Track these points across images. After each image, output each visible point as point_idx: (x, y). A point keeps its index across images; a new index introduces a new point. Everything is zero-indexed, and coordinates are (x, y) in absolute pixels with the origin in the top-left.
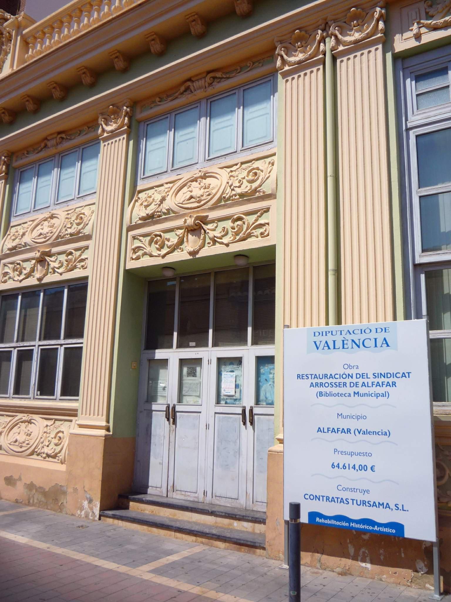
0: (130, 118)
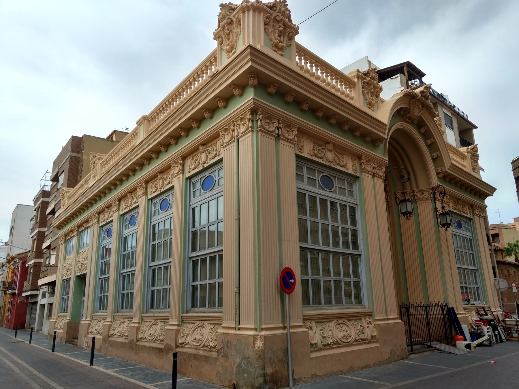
0: (253, 121)
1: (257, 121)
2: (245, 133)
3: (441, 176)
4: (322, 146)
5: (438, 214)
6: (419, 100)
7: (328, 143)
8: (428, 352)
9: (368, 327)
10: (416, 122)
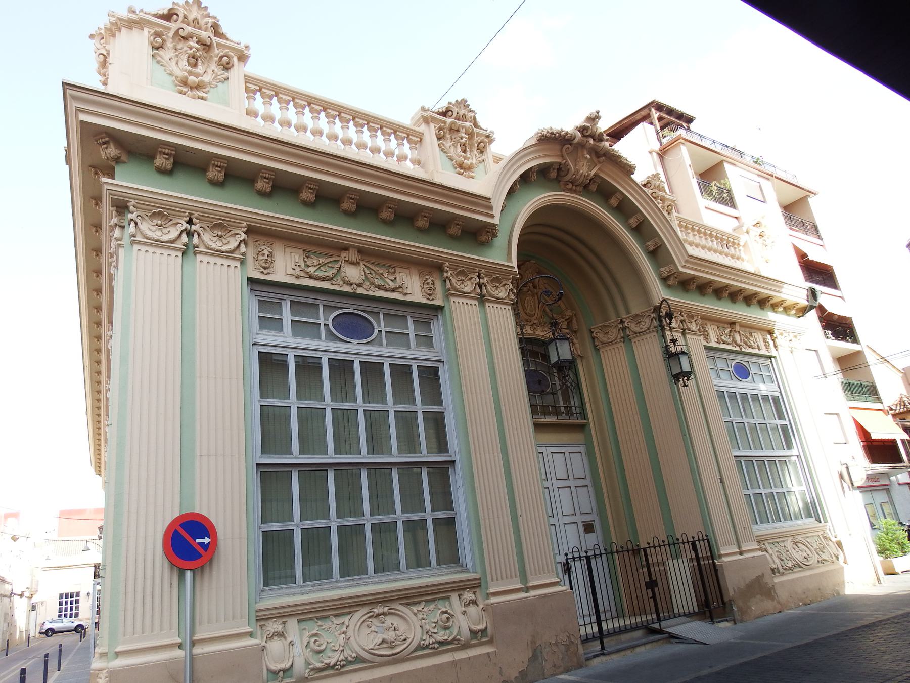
4: (331, 256)
7: (346, 248)
8: (648, 646)
9: (464, 613)
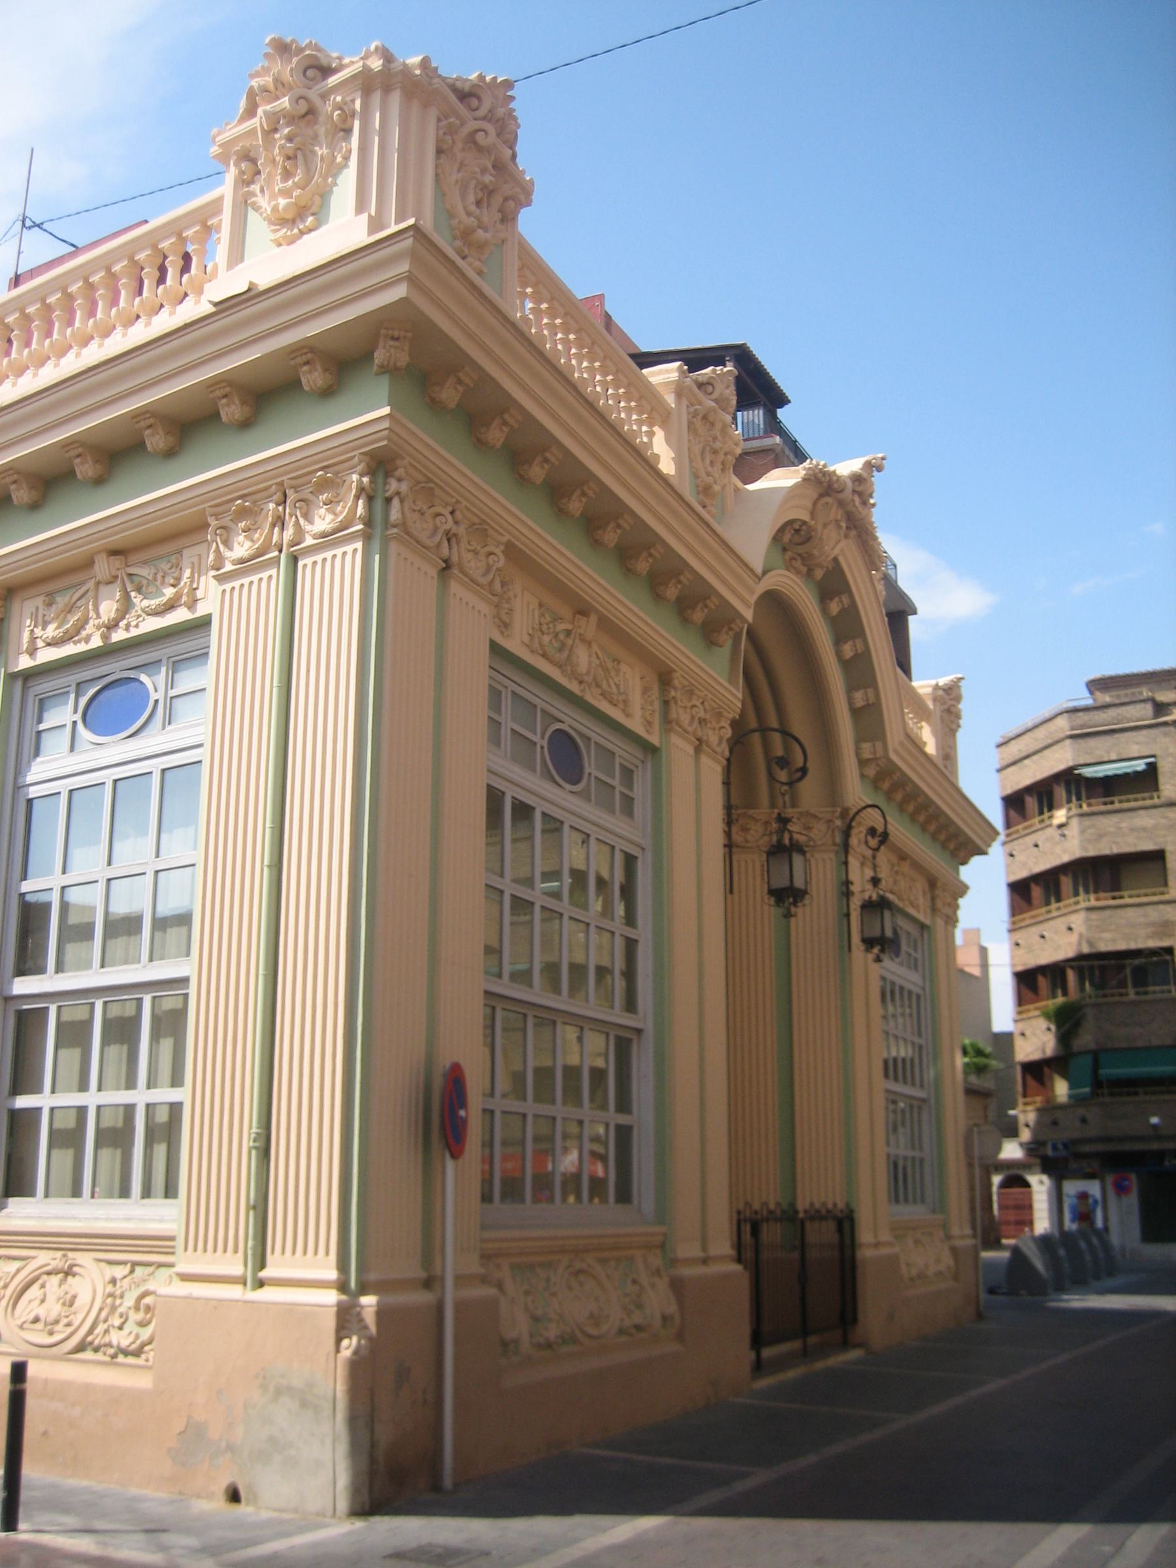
0: (370, 499)
1: (388, 500)
2: (328, 540)
3: (871, 771)
5: (855, 903)
6: (841, 504)
9: (653, 1286)
10: (819, 574)
